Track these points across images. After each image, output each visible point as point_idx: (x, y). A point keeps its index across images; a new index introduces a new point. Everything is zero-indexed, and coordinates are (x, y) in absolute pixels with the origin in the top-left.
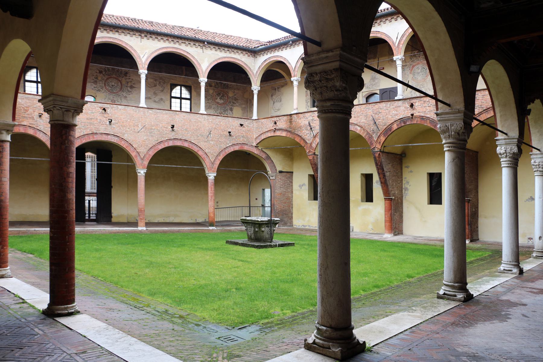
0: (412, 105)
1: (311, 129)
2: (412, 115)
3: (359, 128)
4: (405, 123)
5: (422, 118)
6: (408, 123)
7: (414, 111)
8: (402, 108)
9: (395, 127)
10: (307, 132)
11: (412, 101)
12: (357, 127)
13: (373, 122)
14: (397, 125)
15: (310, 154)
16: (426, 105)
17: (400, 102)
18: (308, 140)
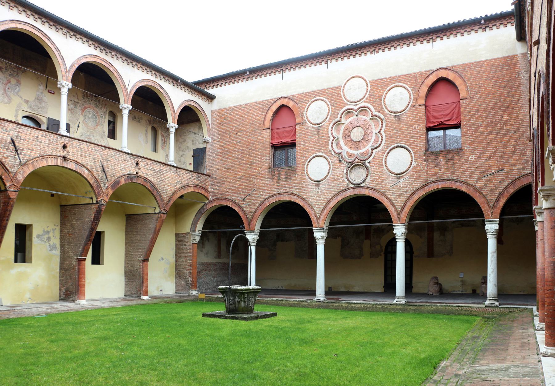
0: (137, 164)
1: (16, 151)
2: (137, 173)
3: (86, 172)
4: (131, 180)
5: (145, 179)
6: (134, 181)
7: (139, 171)
8: (130, 163)
9: (123, 181)
10: (9, 154)
11: (139, 159)
12: (84, 169)
13: (101, 169)
14: (125, 180)
15: (12, 189)
16: (148, 167)
17: (128, 157)
18: (10, 166)
